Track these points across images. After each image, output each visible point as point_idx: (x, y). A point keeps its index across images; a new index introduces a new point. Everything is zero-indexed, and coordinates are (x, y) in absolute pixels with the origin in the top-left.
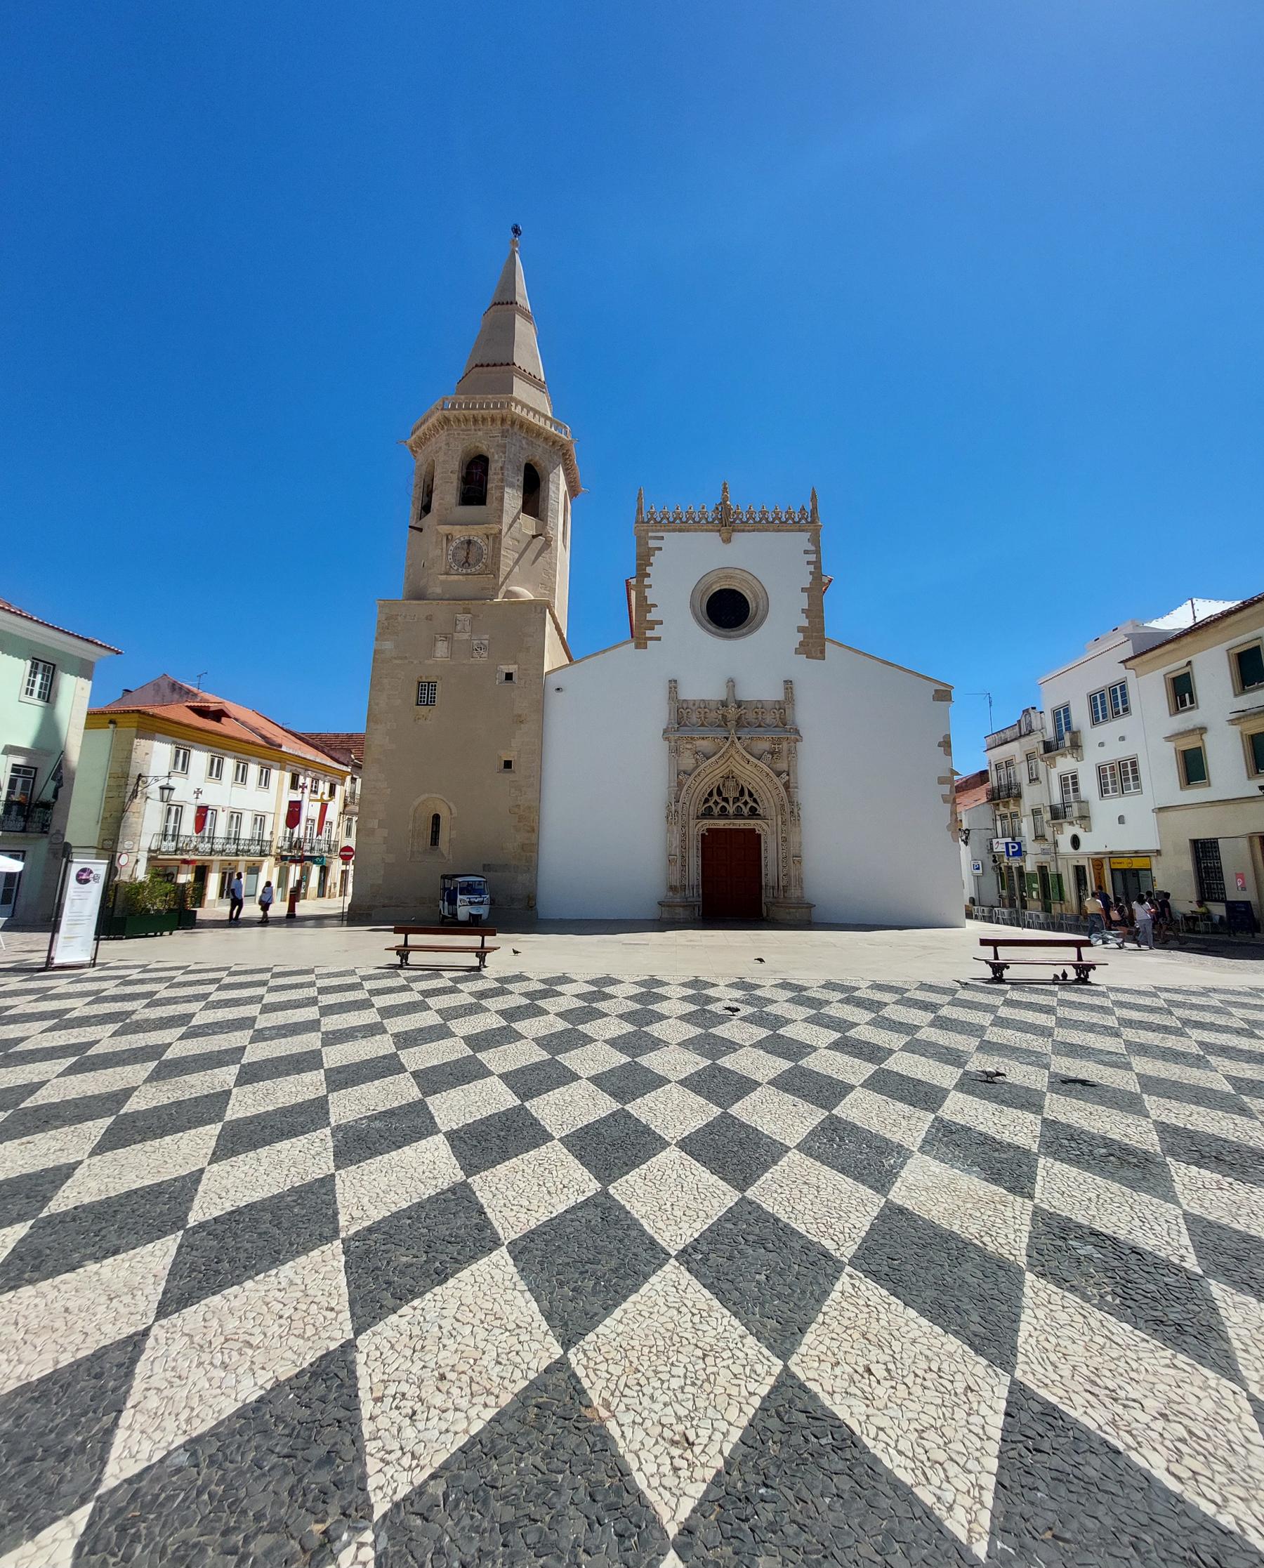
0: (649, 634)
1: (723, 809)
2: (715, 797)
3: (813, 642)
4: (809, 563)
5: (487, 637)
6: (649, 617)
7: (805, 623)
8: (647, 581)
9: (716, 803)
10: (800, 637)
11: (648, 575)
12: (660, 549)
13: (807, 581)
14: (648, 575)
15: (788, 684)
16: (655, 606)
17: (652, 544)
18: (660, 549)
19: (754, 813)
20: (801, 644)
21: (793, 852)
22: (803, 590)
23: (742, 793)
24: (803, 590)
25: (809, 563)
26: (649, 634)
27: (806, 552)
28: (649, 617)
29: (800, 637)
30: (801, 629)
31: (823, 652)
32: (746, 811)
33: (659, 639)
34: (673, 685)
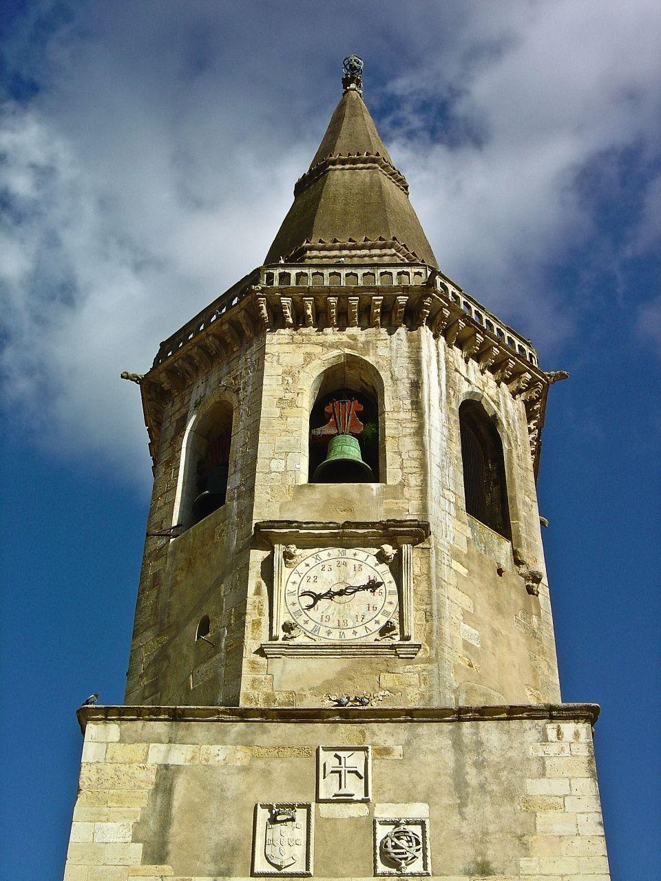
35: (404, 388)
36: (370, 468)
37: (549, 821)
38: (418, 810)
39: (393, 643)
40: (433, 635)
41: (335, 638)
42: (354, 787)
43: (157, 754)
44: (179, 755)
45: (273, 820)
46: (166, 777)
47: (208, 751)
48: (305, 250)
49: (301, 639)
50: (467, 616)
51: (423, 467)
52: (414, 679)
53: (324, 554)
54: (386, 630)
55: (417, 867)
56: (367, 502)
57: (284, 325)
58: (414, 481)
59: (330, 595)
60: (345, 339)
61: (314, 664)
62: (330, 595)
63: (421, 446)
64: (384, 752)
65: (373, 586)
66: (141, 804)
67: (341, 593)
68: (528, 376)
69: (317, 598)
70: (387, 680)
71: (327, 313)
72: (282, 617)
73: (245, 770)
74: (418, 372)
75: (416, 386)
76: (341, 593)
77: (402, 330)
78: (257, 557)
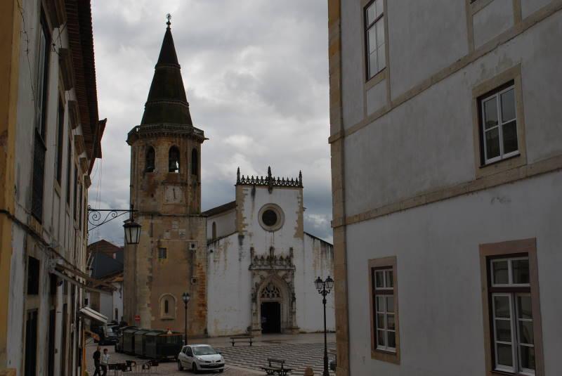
0: (243, 229)
1: (268, 295)
2: (266, 290)
5: (184, 230)
12: (247, 194)
13: (297, 209)
14: (243, 206)
15: (291, 249)
16: (245, 218)
17: (245, 192)
18: (247, 194)
19: (278, 296)
20: (296, 234)
21: (293, 310)
22: (297, 213)
24: (297, 213)
26: (243, 229)
29: (295, 231)
30: (296, 228)
33: (246, 231)
34: (252, 249)
37: (201, 232)
42: (177, 227)
43: (150, 221)
44: (153, 222)
46: (152, 224)
47: (157, 221)
54: (181, 201)
64: (180, 221)
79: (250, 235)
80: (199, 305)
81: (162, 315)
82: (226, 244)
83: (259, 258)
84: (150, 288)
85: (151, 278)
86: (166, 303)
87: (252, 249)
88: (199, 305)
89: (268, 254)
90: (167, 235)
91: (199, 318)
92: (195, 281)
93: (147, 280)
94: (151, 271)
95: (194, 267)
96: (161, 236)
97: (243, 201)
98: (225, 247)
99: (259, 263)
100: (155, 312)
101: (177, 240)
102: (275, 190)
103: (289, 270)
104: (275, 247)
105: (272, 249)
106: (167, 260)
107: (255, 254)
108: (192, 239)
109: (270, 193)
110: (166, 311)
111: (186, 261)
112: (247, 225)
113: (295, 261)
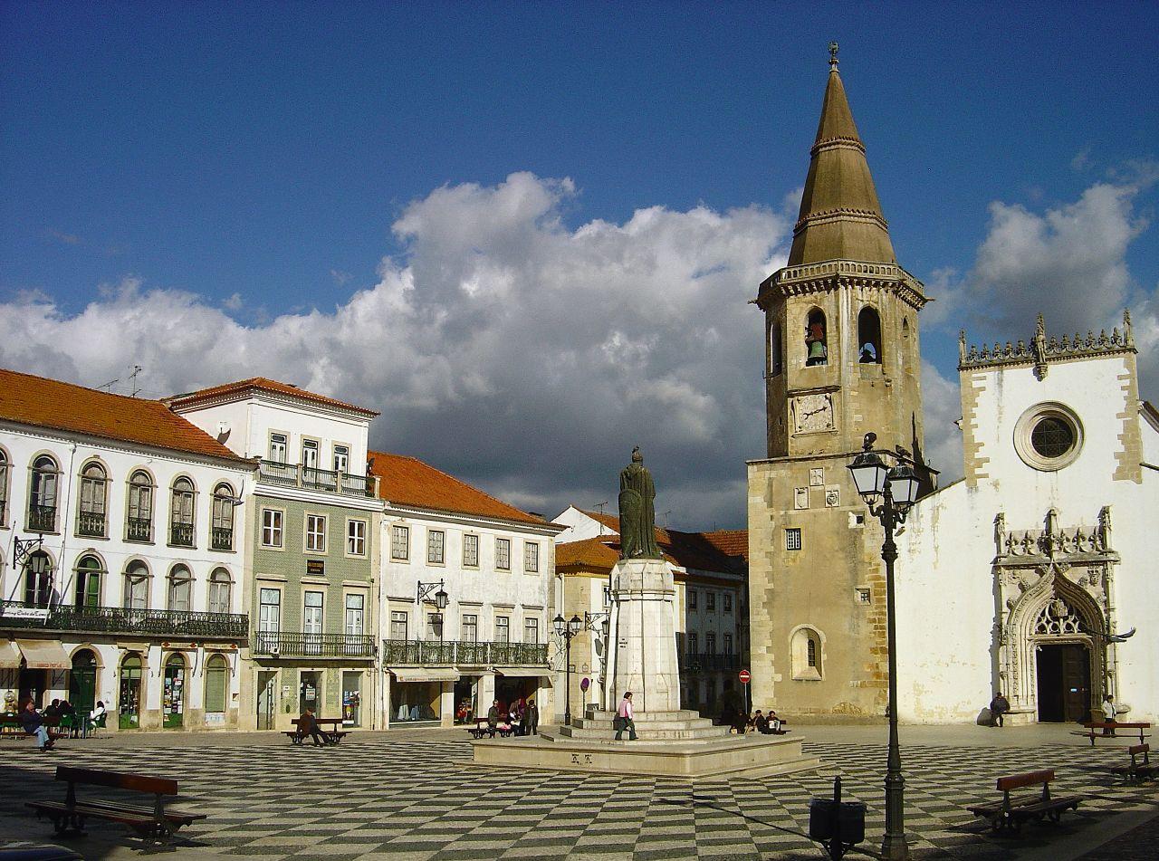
0: (978, 471)
1: (1055, 627)
3: (1131, 465)
4: (1123, 388)
5: (837, 487)
6: (977, 455)
7: (1121, 449)
8: (973, 421)
9: (1048, 622)
10: (1117, 463)
11: (974, 416)
12: (983, 389)
14: (974, 416)
17: (976, 384)
18: (983, 389)
20: (1119, 470)
22: (1119, 416)
23: (1070, 613)
24: (1119, 416)
25: (1123, 388)
26: (978, 471)
27: (1120, 378)
28: (977, 455)
29: (1117, 463)
30: (1117, 456)
31: (1139, 475)
32: (1076, 627)
33: (985, 476)
34: (999, 518)
35: (834, 319)
36: (823, 359)
38: (837, 487)
39: (829, 432)
40: (843, 424)
41: (814, 430)
44: (773, 475)
45: (799, 493)
47: (781, 472)
48: (807, 222)
49: (804, 431)
50: (857, 412)
51: (840, 357)
52: (837, 442)
53: (809, 397)
55: (836, 504)
56: (824, 375)
57: (792, 295)
58: (837, 364)
59: (812, 414)
60: (813, 298)
61: (807, 439)
62: (812, 414)
63: (839, 347)
64: (829, 468)
65: (824, 409)
66: (765, 490)
67: (815, 412)
68: (891, 284)
69: (808, 415)
70: (829, 443)
71: (805, 287)
72: (798, 424)
73: (791, 477)
74: (838, 313)
75: (837, 318)
76: (815, 412)
77: (832, 291)
78: (790, 400)
79: (996, 485)
80: (874, 651)
81: (800, 666)
82: (936, 509)
83: (1020, 538)
84: (768, 613)
85: (771, 592)
86: (813, 645)
87: (999, 518)
88: (874, 651)
89: (1043, 527)
90: (803, 500)
91: (874, 679)
92: (867, 595)
93: (765, 598)
94: (772, 580)
95: (859, 567)
96: (789, 504)
97: (977, 405)
98: (935, 519)
99: (1019, 550)
100: (782, 664)
101: (824, 510)
102: (1055, 370)
103: (1098, 563)
104: (1058, 506)
105: (1050, 516)
106: (801, 554)
107: (1007, 529)
108: (854, 504)
109: (1040, 379)
110: (814, 659)
111: (841, 555)
112: (987, 460)
113: (1113, 541)
